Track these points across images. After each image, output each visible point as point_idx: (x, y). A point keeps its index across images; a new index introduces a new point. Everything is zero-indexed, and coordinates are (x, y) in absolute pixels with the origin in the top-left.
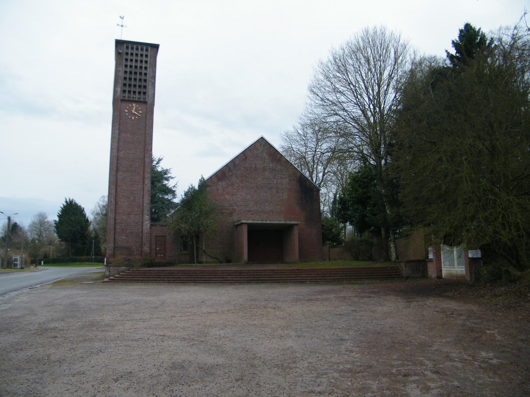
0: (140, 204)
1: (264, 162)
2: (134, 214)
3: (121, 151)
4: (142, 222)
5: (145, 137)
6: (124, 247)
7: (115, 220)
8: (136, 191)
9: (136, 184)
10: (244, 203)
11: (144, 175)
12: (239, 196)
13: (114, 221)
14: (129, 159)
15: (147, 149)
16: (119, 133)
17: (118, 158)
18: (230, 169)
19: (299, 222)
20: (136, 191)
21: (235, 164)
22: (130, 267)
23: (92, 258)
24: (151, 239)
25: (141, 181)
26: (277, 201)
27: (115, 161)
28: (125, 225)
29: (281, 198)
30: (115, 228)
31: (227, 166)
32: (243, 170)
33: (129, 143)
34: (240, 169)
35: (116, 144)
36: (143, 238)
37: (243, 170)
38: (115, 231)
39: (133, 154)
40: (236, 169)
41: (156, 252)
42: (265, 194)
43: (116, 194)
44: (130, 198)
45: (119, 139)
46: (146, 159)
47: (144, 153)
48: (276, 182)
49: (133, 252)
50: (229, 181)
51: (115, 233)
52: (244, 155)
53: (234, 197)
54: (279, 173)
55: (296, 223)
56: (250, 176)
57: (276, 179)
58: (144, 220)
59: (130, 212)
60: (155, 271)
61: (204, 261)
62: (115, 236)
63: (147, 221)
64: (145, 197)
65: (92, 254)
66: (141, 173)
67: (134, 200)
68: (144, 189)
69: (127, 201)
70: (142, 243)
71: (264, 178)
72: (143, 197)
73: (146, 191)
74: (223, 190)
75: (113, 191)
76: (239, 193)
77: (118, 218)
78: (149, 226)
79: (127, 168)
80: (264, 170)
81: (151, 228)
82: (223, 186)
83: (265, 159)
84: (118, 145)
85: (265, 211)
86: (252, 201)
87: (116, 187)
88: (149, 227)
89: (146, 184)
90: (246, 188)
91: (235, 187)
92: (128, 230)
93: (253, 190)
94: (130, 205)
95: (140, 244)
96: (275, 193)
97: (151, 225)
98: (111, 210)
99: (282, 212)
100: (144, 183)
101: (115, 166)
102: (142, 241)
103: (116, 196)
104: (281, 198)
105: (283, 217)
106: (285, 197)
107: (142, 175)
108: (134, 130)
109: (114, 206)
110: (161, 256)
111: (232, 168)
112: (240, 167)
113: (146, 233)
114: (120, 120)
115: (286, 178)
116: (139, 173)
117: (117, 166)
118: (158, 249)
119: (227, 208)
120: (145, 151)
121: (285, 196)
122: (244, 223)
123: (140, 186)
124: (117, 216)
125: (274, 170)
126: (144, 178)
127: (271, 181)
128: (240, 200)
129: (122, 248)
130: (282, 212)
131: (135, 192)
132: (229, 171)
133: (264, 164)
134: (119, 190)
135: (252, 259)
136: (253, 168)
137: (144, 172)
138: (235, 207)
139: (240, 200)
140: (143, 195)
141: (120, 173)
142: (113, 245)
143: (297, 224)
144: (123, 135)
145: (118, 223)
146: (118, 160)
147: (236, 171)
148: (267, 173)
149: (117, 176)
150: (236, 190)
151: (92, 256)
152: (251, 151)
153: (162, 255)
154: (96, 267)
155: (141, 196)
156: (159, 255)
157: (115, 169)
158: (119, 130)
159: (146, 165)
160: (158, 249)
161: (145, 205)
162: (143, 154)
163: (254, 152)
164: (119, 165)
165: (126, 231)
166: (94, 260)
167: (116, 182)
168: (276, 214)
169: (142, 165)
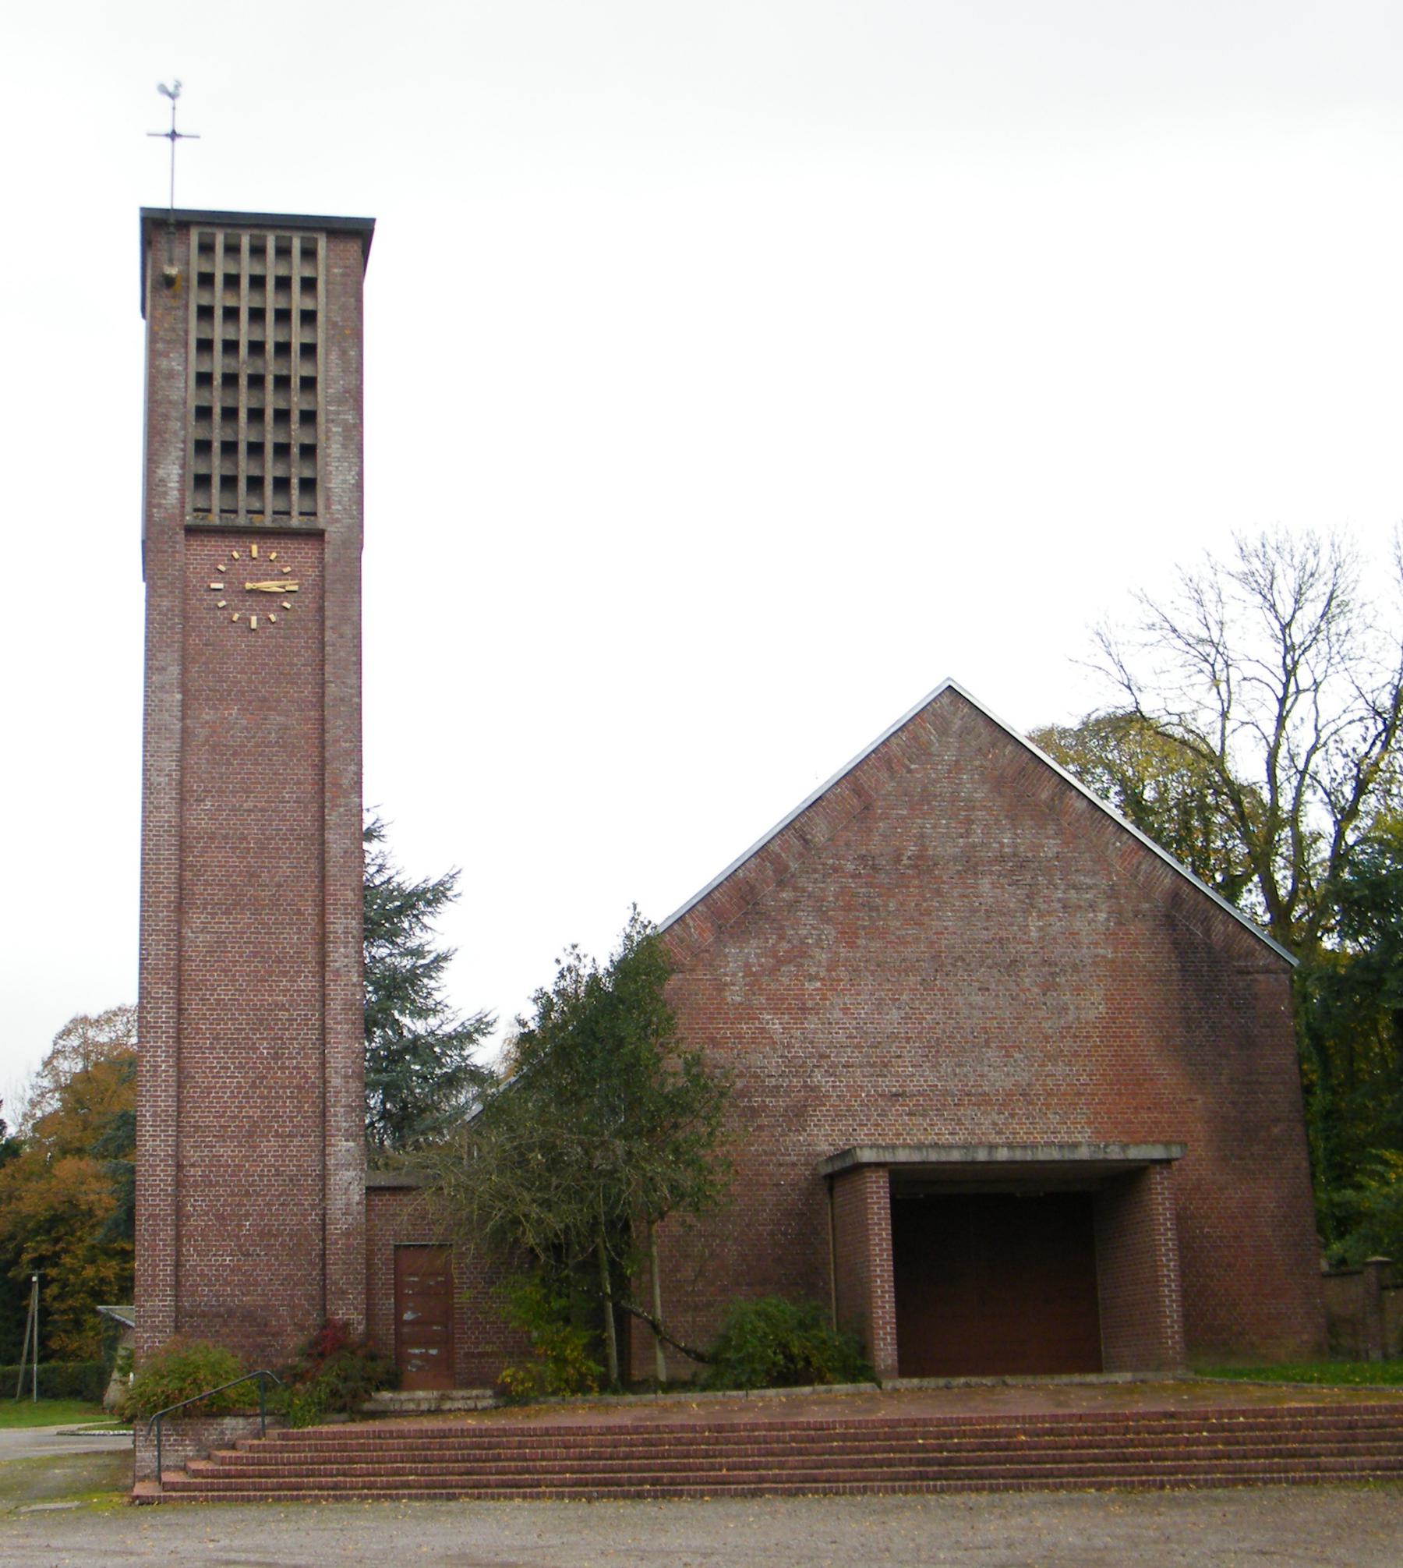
0: (305, 1077)
1: (969, 821)
2: (277, 1135)
3: (199, 801)
4: (323, 1177)
5: (322, 720)
6: (231, 1313)
7: (179, 1166)
8: (283, 1008)
9: (285, 974)
10: (868, 1056)
11: (322, 922)
12: (837, 1014)
13: (171, 1171)
14: (243, 838)
15: (337, 785)
16: (184, 705)
17: (182, 838)
18: (781, 869)
19: (1175, 1152)
20: (283, 1008)
21: (806, 841)
22: (268, 1419)
23: (28, 1373)
24: (369, 1265)
25: (311, 952)
26: (1047, 1038)
27: (169, 853)
28: (233, 1194)
29: (1071, 1017)
30: (179, 1209)
31: (763, 853)
32: (855, 876)
33: (235, 754)
34: (835, 870)
35: (170, 764)
36: (331, 1259)
37: (855, 876)
38: (178, 1228)
39: (263, 810)
40: (815, 871)
41: (397, 1332)
42: (978, 999)
43: (179, 1030)
44: (255, 1049)
45: (185, 734)
46: (330, 836)
47: (322, 807)
48: (1041, 929)
49: (275, 1335)
50: (781, 938)
51: (178, 1237)
52: (858, 791)
53: (812, 1023)
54: (1050, 882)
55: (1158, 1153)
56: (892, 906)
57: (1040, 916)
58: (331, 1162)
59: (255, 1125)
60: (401, 1435)
61: (663, 1378)
62: (178, 1252)
63: (347, 1166)
64: (331, 1038)
65: (30, 1353)
66: (310, 910)
67: (276, 1056)
68: (324, 999)
69: (241, 1067)
70: (324, 1287)
71: (974, 911)
72: (323, 1040)
73: (335, 1006)
74: (751, 985)
75: (166, 1011)
76: (835, 1000)
77: (192, 1154)
78: (356, 1195)
79: (234, 886)
80: (970, 865)
81: (369, 1208)
82: (747, 965)
83: (974, 808)
84: (182, 768)
85: (985, 1094)
86: (908, 1039)
87: (179, 991)
88: (357, 1198)
89: (337, 972)
90: (873, 973)
91: (813, 970)
92: (247, 1215)
93: (912, 979)
94: (253, 1086)
95: (315, 1290)
96: (1036, 990)
97: (371, 1190)
98: (155, 1115)
99: (1079, 1094)
100: (323, 964)
101: (168, 877)
102: (324, 1274)
103: (178, 1040)
104: (1071, 1017)
105: (1089, 1123)
106: (1091, 1015)
107: (312, 921)
108: (263, 683)
109: (172, 1091)
110: (425, 1357)
111: (794, 866)
112: (836, 856)
113: (347, 1234)
114: (185, 634)
115: (1092, 907)
116: (299, 912)
117: (180, 879)
118: (408, 1316)
119: (773, 1081)
120: (322, 791)
121: (1092, 1006)
122: (869, 1165)
123: (307, 983)
124: (188, 1143)
125: (1023, 865)
126: (322, 940)
127: (1011, 925)
128: (841, 1037)
129: (218, 1315)
130: (1079, 1094)
131: (284, 1015)
132: (781, 884)
133: (967, 834)
134: (193, 1008)
135: (908, 1365)
136: (905, 862)
137: (322, 905)
138: (818, 1077)
139: (841, 1037)
140: (323, 1029)
141: (197, 918)
142: (169, 1301)
143: (1166, 1162)
144: (208, 715)
145: (196, 1185)
146: (183, 846)
147: (815, 881)
148: (985, 884)
149: (180, 936)
150: (818, 984)
151: (29, 1361)
152: (890, 768)
153: (433, 1352)
154: (53, 1430)
155: (314, 1035)
156: (417, 1351)
157: (169, 896)
158: (184, 691)
159: (332, 870)
160: (408, 1316)
161: (336, 1082)
162: (314, 808)
163: (910, 771)
164: (188, 875)
165: (240, 1226)
166: (40, 1383)
167: (179, 968)
168: (1048, 1106)
169: (313, 866)
